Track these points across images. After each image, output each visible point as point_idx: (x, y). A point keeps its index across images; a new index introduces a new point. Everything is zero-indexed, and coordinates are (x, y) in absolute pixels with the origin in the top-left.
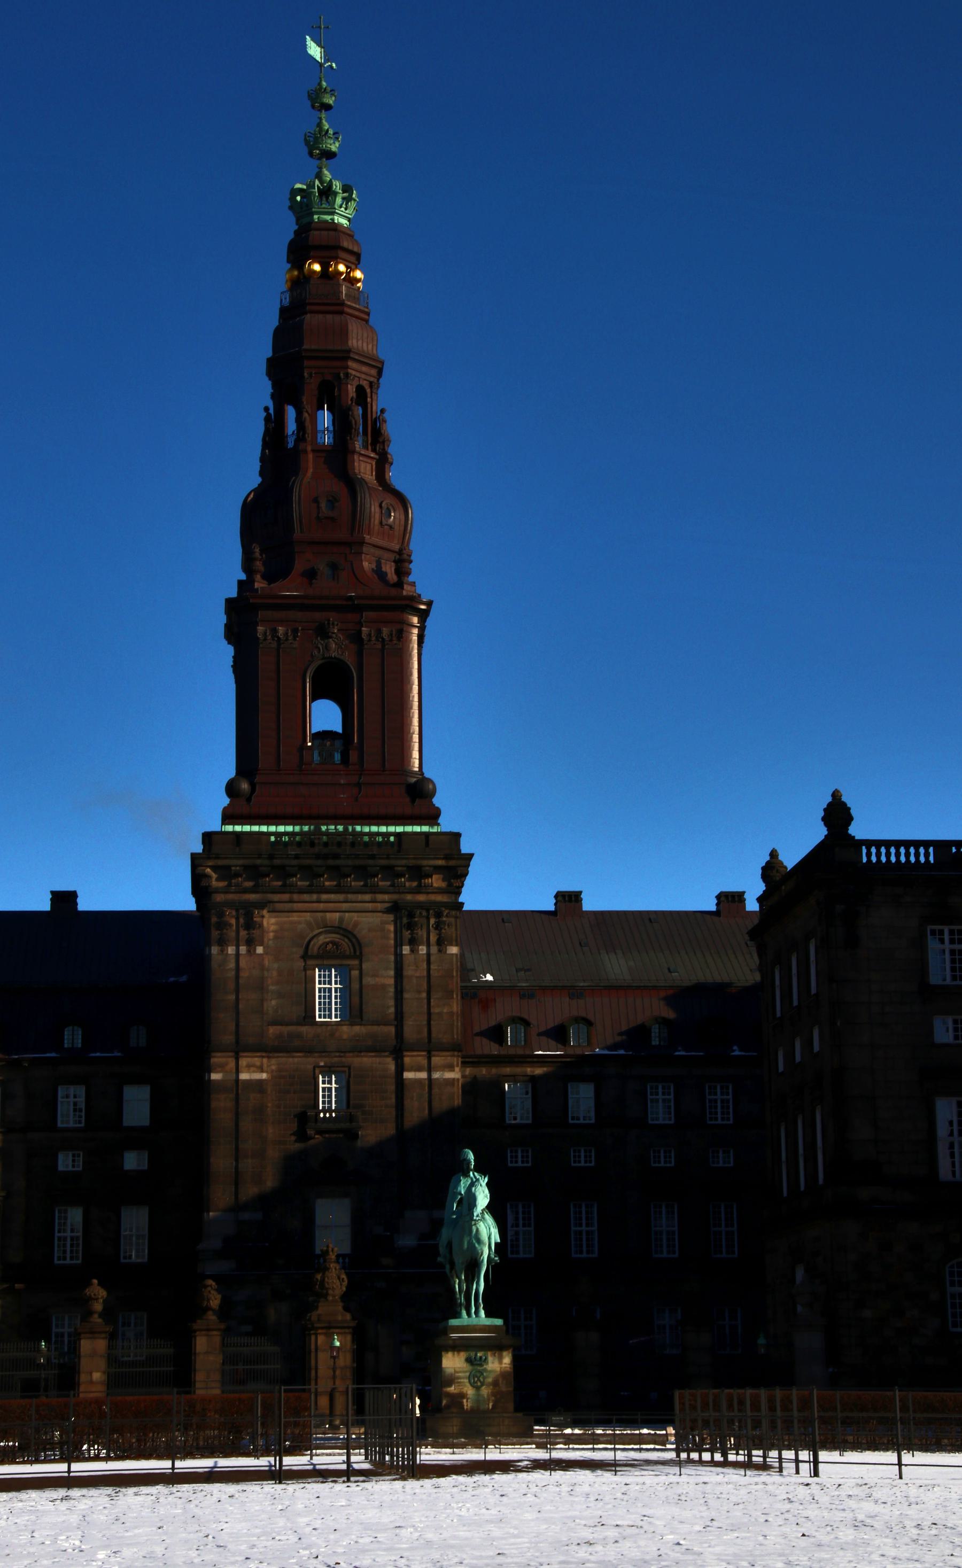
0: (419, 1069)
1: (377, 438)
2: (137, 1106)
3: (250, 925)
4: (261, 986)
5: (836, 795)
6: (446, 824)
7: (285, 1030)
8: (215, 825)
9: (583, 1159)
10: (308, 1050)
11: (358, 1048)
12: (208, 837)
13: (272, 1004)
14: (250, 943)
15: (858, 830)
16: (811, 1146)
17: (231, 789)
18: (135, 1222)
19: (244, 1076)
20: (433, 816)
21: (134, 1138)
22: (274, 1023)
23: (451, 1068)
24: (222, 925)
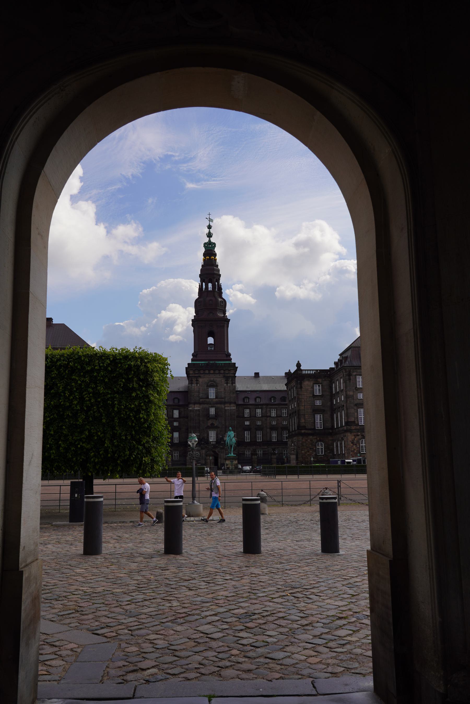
0: (228, 407)
1: (220, 289)
2: (176, 414)
3: (197, 380)
4: (199, 392)
5: (298, 362)
6: (233, 361)
7: (203, 400)
8: (190, 362)
9: (259, 423)
10: (207, 404)
11: (217, 403)
12: (188, 364)
13: (201, 395)
14: (197, 384)
15: (302, 368)
16: (295, 423)
17: (193, 355)
18: (176, 435)
19: (196, 408)
20: (231, 360)
21: (176, 420)
22: (201, 399)
23: (234, 407)
24: (192, 380)
